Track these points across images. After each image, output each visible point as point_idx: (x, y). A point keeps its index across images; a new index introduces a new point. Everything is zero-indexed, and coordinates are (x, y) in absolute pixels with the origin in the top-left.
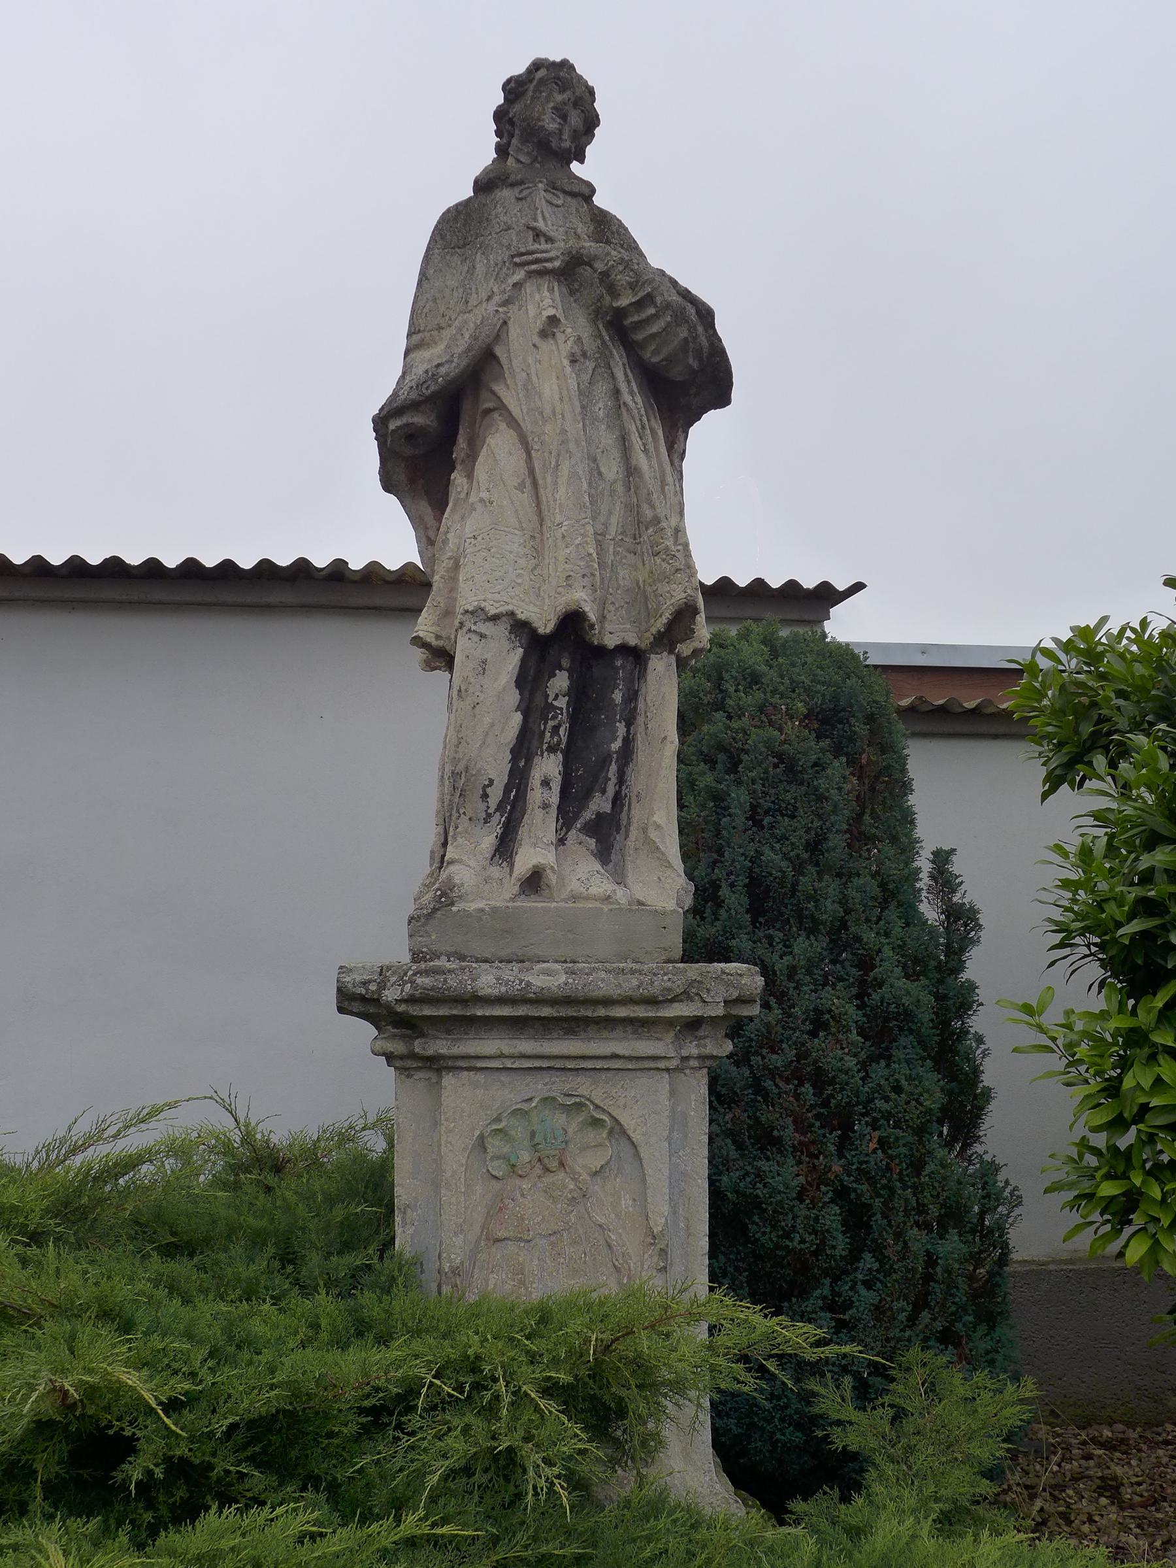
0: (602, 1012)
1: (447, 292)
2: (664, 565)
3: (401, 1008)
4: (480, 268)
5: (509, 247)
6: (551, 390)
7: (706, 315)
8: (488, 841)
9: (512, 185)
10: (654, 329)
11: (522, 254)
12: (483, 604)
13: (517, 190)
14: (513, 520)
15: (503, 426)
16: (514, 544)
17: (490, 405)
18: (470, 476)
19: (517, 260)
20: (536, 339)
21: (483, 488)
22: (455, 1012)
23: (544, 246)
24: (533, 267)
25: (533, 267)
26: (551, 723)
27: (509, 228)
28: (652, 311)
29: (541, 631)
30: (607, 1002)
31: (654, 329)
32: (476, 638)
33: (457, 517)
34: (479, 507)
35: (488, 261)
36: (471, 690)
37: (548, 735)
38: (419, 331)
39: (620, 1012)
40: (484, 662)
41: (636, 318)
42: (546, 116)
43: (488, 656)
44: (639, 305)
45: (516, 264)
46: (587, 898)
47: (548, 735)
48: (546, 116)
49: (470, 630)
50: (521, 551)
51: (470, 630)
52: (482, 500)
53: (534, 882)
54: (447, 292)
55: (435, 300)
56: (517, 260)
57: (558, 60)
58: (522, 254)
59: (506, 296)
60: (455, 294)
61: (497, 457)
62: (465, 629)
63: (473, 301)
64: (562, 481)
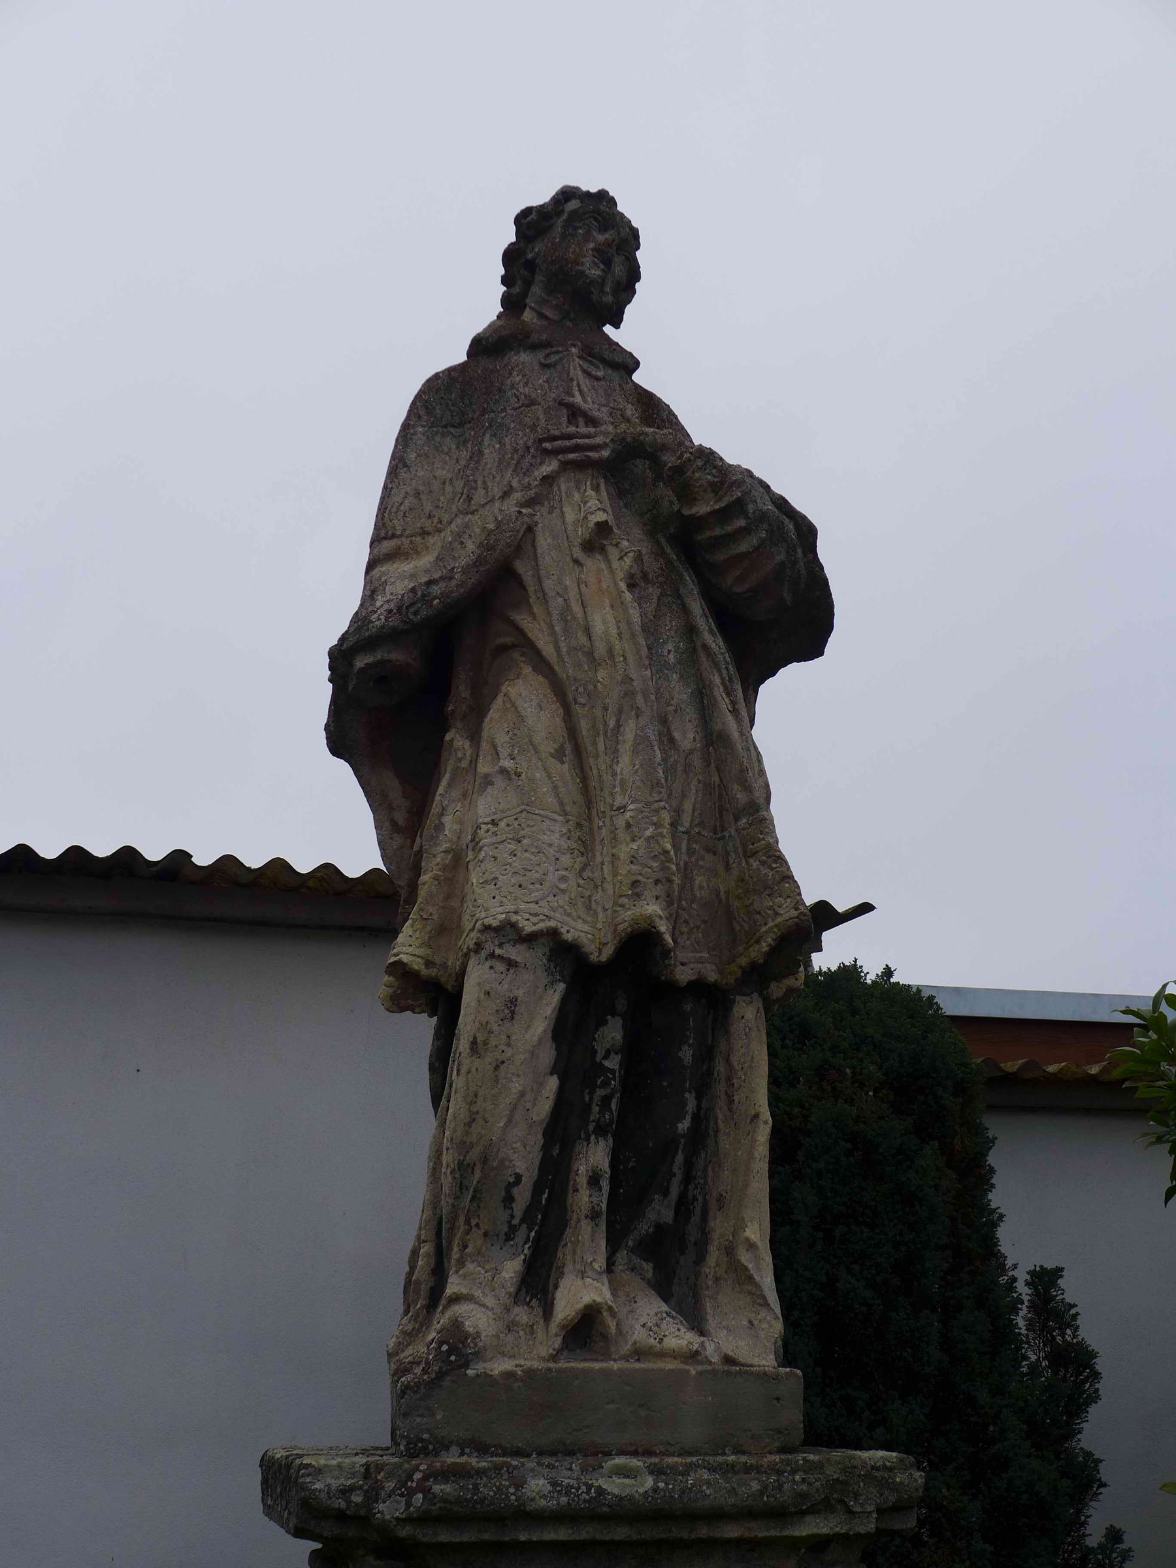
0: (703, 1532)
1: (436, 485)
2: (764, 870)
3: (404, 1532)
4: (490, 455)
5: (534, 428)
6: (605, 622)
7: (807, 533)
8: (511, 1269)
9: (534, 347)
10: (743, 547)
11: (555, 438)
12: (514, 918)
13: (540, 355)
14: (551, 800)
15: (527, 670)
16: (554, 834)
17: (508, 640)
18: (475, 736)
19: (547, 445)
20: (578, 553)
21: (504, 753)
22: (486, 1536)
23: (583, 430)
24: (572, 456)
25: (572, 456)
26: (600, 1093)
27: (532, 403)
28: (741, 523)
29: (593, 958)
30: (717, 1515)
31: (743, 547)
32: (500, 967)
33: (456, 794)
34: (499, 781)
35: (502, 444)
36: (493, 1042)
37: (596, 1109)
38: (393, 536)
39: (732, 1531)
40: (514, 1001)
41: (718, 532)
42: (573, 261)
43: (520, 993)
44: (724, 515)
45: (547, 452)
46: (662, 1355)
47: (596, 1109)
48: (573, 261)
49: (492, 955)
50: (565, 844)
51: (492, 955)
52: (503, 771)
53: (585, 1331)
54: (436, 485)
55: (417, 495)
56: (547, 445)
57: (593, 190)
58: (555, 438)
59: (532, 493)
60: (448, 488)
61: (522, 709)
62: (483, 954)
63: (479, 497)
64: (626, 747)
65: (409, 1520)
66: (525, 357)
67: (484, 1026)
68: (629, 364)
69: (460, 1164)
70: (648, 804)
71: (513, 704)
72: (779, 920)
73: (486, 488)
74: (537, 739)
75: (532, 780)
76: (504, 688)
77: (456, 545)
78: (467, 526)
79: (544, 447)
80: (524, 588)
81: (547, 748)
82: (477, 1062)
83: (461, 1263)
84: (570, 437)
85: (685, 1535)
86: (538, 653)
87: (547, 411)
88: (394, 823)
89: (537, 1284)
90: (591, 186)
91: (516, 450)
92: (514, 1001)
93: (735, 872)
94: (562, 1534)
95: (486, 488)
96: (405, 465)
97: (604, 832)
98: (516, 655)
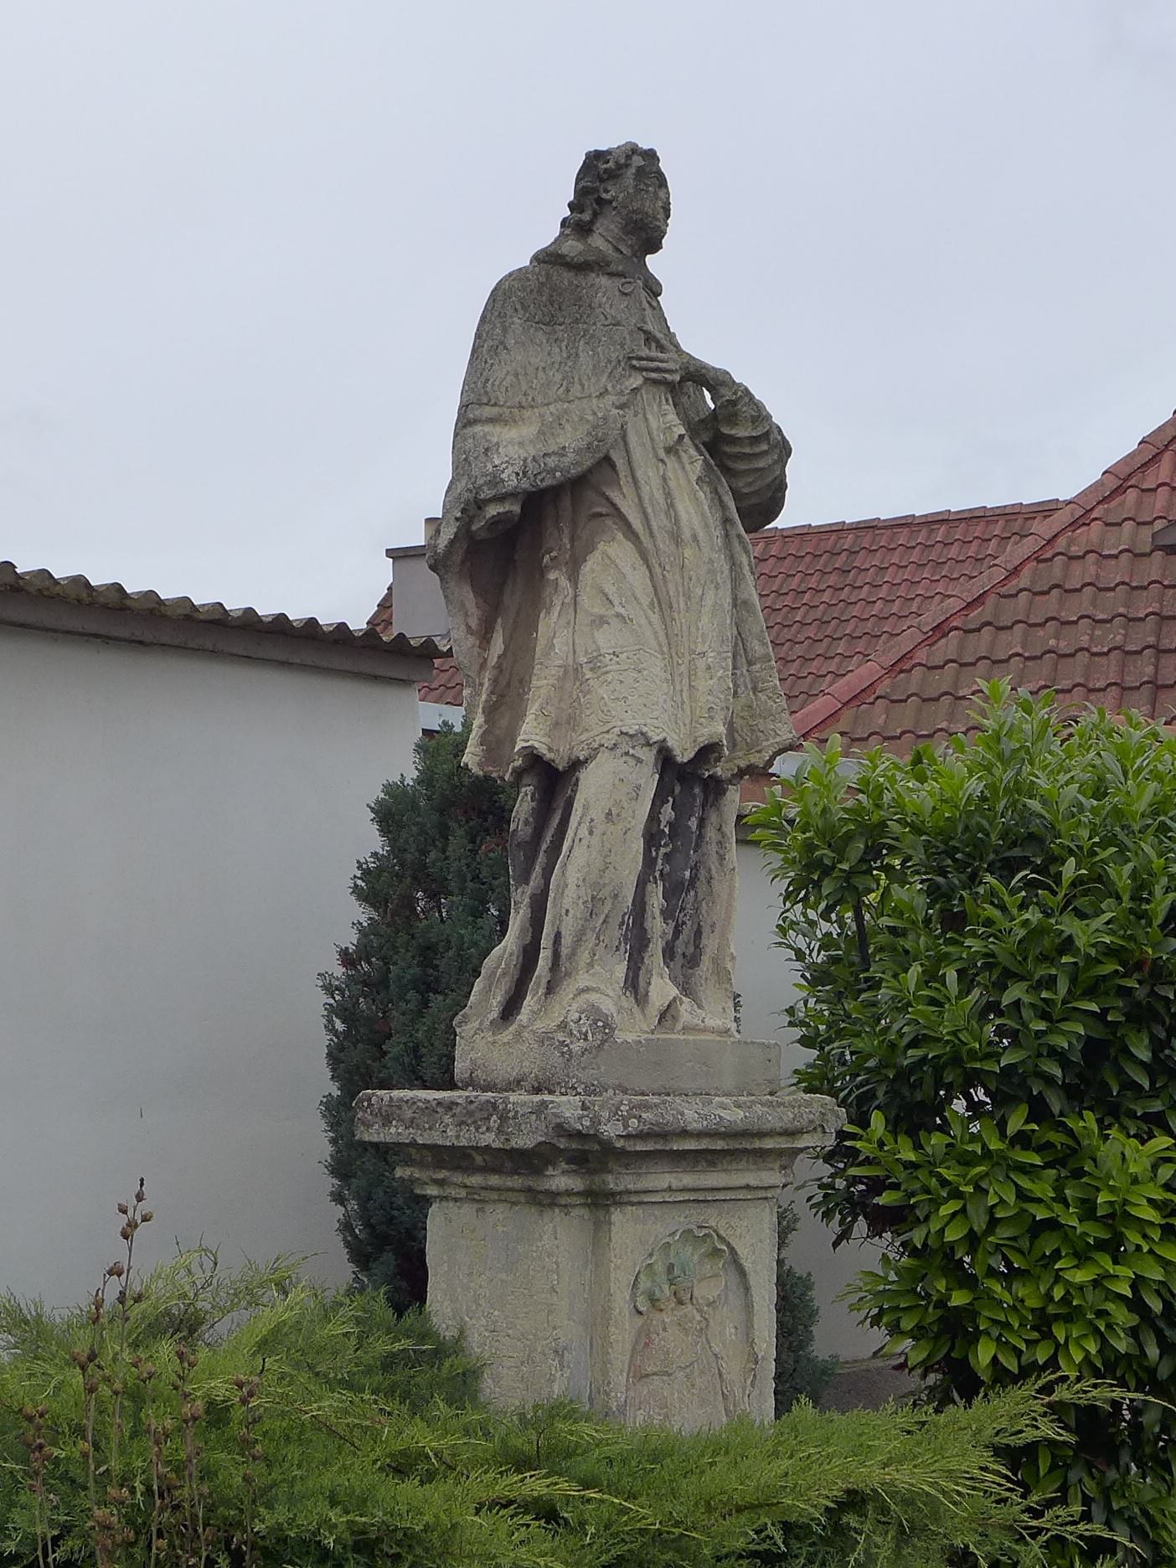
0: (757, 1144)
1: (530, 370)
2: (770, 703)
3: (619, 1144)
4: (585, 358)
5: (622, 345)
6: (687, 512)
7: (785, 450)
8: (621, 970)
9: (611, 275)
10: (761, 464)
11: (641, 359)
12: (645, 729)
13: (619, 282)
14: (654, 643)
15: (620, 536)
16: (656, 667)
17: (603, 510)
18: (574, 578)
19: (634, 362)
20: (662, 454)
21: (616, 602)
22: (658, 1147)
23: (654, 354)
24: (653, 375)
25: (653, 375)
26: (663, 850)
27: (618, 324)
28: (765, 447)
29: (679, 759)
30: (771, 1134)
31: (761, 464)
32: (632, 762)
33: (563, 621)
34: (614, 621)
35: (596, 354)
36: (623, 815)
37: (660, 862)
38: (495, 405)
39: (769, 1144)
40: (638, 787)
41: (747, 450)
42: (620, 201)
43: (642, 782)
44: (754, 440)
45: (634, 367)
46: (704, 1030)
47: (660, 862)
48: (620, 201)
49: (627, 754)
50: (664, 675)
51: (627, 754)
52: (618, 615)
53: (667, 1015)
54: (530, 370)
55: (516, 375)
56: (634, 362)
57: (645, 147)
58: (641, 359)
59: (624, 399)
60: (541, 374)
61: (611, 566)
62: (619, 752)
63: (576, 390)
64: (706, 610)
65: (628, 1137)
66: (604, 281)
67: (618, 803)
68: (653, 289)
69: (593, 898)
70: (719, 653)
71: (613, 562)
72: (778, 739)
73: (583, 386)
74: (638, 593)
75: (640, 626)
76: (601, 546)
77: (556, 425)
78: (566, 411)
79: (632, 363)
80: (616, 472)
81: (645, 601)
82: (612, 828)
83: (591, 965)
84: (652, 360)
85: (748, 1146)
86: (628, 525)
87: (631, 333)
88: (469, 627)
89: (634, 984)
90: (644, 145)
91: (610, 361)
92: (638, 787)
93: (743, 700)
94: (704, 1144)
95: (583, 386)
96: (505, 348)
97: (683, 668)
98: (609, 522)
